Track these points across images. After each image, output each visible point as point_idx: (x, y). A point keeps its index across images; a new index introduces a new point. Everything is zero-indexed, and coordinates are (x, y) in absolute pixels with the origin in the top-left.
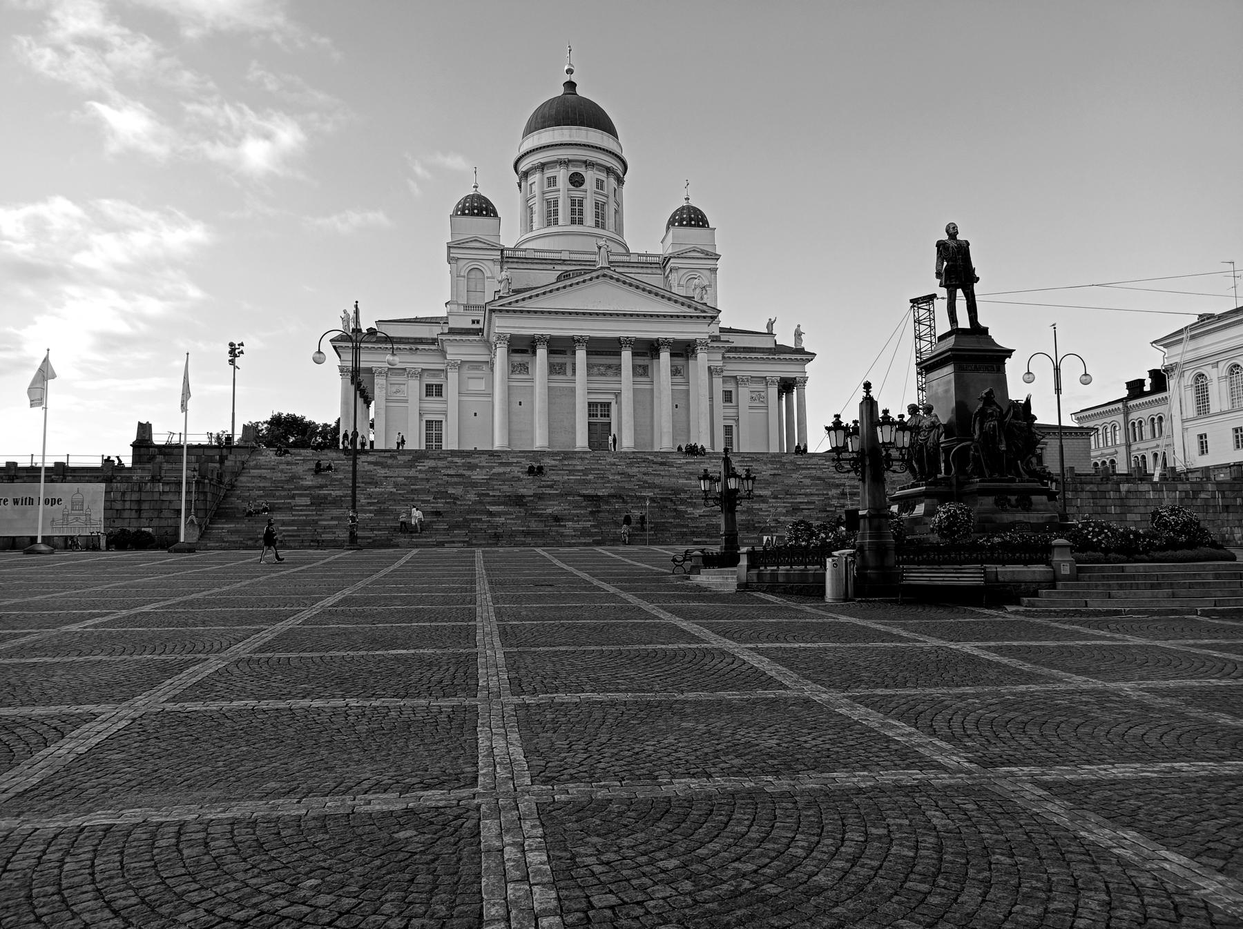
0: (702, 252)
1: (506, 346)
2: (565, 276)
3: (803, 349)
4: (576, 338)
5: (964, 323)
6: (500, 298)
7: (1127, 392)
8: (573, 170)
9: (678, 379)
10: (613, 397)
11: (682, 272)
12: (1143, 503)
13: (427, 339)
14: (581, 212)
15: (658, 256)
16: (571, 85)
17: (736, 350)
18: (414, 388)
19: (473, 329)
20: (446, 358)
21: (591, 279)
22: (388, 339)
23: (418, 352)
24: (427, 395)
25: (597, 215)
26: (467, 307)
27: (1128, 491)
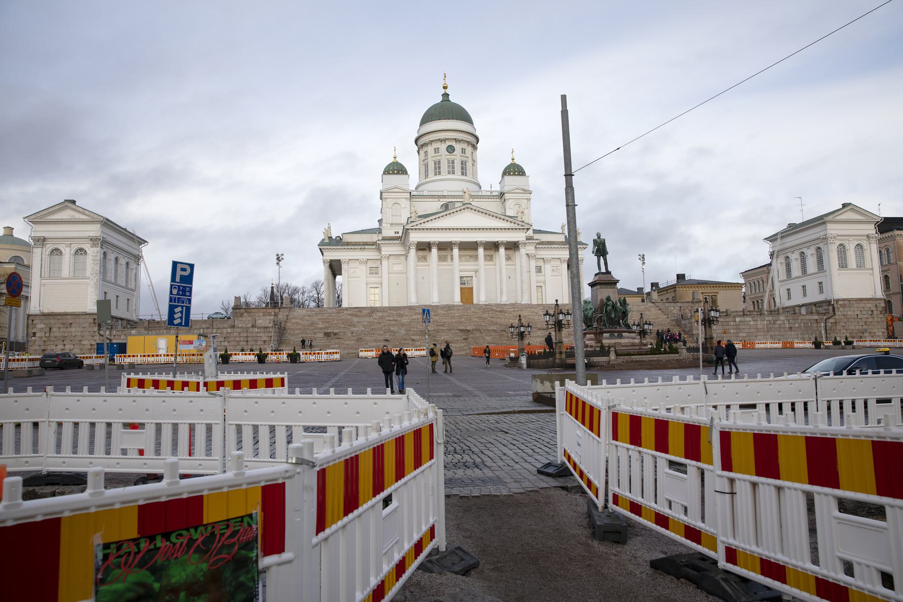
0: (522, 189)
2: (446, 207)
4: (453, 242)
5: (603, 270)
6: (412, 222)
8: (448, 143)
9: (509, 262)
10: (474, 273)
11: (511, 201)
12: (748, 327)
13: (369, 242)
14: (453, 167)
16: (446, 96)
17: (542, 243)
20: (381, 254)
22: (348, 244)
25: (462, 168)
27: (741, 321)
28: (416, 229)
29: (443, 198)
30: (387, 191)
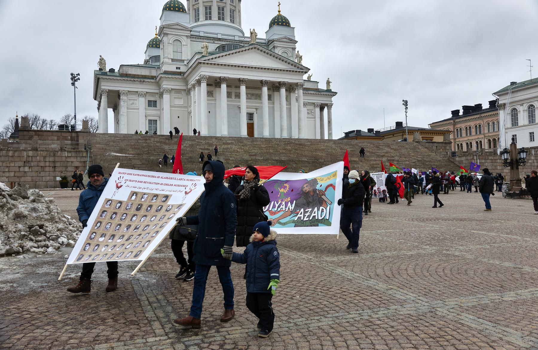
0: (289, 39)
1: (206, 82)
3: (331, 90)
7: (452, 115)
10: (255, 110)
11: (279, 49)
13: (148, 76)
14: (223, 14)
15: (265, 40)
18: (142, 102)
19: (177, 72)
21: (245, 50)
22: (127, 75)
23: (144, 83)
24: (148, 106)
26: (173, 60)
28: (208, 63)
29: (217, 40)
30: (169, 27)
